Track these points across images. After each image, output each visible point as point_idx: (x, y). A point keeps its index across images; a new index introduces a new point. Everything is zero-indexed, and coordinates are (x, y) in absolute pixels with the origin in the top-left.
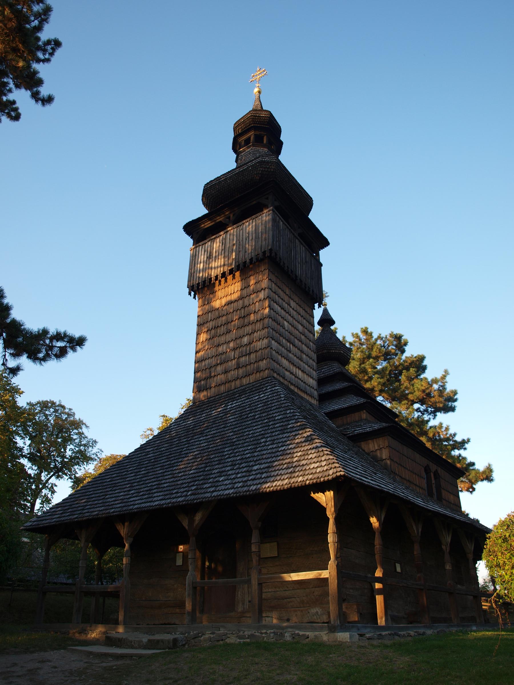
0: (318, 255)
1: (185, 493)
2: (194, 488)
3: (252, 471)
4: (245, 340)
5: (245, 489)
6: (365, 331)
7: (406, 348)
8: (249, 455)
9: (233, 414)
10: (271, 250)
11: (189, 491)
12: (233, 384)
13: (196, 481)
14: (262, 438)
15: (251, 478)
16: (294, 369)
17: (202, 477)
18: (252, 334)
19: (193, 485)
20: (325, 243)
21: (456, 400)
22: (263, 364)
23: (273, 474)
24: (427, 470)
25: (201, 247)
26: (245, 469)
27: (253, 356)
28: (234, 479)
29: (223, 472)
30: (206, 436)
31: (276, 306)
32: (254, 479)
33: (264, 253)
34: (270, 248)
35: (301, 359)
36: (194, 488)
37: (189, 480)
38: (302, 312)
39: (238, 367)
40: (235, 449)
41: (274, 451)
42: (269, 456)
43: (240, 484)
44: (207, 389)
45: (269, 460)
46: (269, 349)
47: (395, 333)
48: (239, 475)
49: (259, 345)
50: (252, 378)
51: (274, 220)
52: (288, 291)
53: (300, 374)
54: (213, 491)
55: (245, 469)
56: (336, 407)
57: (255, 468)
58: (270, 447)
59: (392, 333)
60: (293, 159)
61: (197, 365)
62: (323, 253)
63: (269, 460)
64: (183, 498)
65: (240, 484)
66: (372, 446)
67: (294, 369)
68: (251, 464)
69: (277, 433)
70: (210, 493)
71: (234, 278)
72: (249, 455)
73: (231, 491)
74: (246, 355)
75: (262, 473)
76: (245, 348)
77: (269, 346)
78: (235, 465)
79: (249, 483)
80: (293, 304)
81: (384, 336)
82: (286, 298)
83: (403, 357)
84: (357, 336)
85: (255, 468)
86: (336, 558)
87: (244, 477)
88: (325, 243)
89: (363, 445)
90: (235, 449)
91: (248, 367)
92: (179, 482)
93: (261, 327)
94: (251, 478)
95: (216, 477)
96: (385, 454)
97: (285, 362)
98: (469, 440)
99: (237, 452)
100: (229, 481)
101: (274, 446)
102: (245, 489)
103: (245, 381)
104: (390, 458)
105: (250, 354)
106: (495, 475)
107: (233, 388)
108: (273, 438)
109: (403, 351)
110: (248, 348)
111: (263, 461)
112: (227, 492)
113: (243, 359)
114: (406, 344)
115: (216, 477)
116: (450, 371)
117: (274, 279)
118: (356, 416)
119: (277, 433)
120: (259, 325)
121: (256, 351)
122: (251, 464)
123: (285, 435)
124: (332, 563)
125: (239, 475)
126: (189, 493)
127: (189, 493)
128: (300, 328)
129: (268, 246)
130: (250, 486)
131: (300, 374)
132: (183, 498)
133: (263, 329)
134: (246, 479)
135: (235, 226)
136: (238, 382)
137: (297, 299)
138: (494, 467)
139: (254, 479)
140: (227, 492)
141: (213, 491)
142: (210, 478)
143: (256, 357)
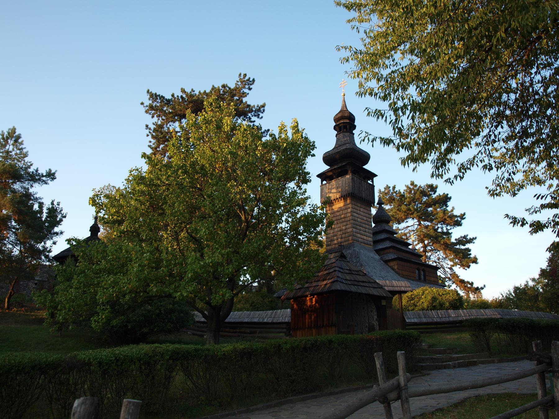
0: (373, 181)
4: (344, 228)
6: (412, 183)
7: (438, 190)
16: (362, 237)
20: (376, 176)
21: (464, 218)
22: (350, 238)
24: (418, 269)
31: (355, 214)
35: (366, 232)
38: (366, 211)
39: (342, 238)
51: (352, 179)
52: (359, 205)
53: (365, 237)
56: (381, 247)
62: (375, 179)
66: (392, 264)
67: (362, 237)
77: (352, 231)
80: (362, 210)
82: (359, 208)
83: (434, 196)
84: (407, 187)
88: (376, 176)
89: (389, 263)
96: (396, 267)
97: (359, 235)
98: (476, 238)
104: (398, 269)
106: (478, 261)
113: (343, 236)
114: (437, 187)
116: (455, 208)
117: (353, 202)
118: (388, 251)
120: (348, 223)
128: (365, 218)
131: (365, 237)
137: (363, 207)
138: (477, 257)
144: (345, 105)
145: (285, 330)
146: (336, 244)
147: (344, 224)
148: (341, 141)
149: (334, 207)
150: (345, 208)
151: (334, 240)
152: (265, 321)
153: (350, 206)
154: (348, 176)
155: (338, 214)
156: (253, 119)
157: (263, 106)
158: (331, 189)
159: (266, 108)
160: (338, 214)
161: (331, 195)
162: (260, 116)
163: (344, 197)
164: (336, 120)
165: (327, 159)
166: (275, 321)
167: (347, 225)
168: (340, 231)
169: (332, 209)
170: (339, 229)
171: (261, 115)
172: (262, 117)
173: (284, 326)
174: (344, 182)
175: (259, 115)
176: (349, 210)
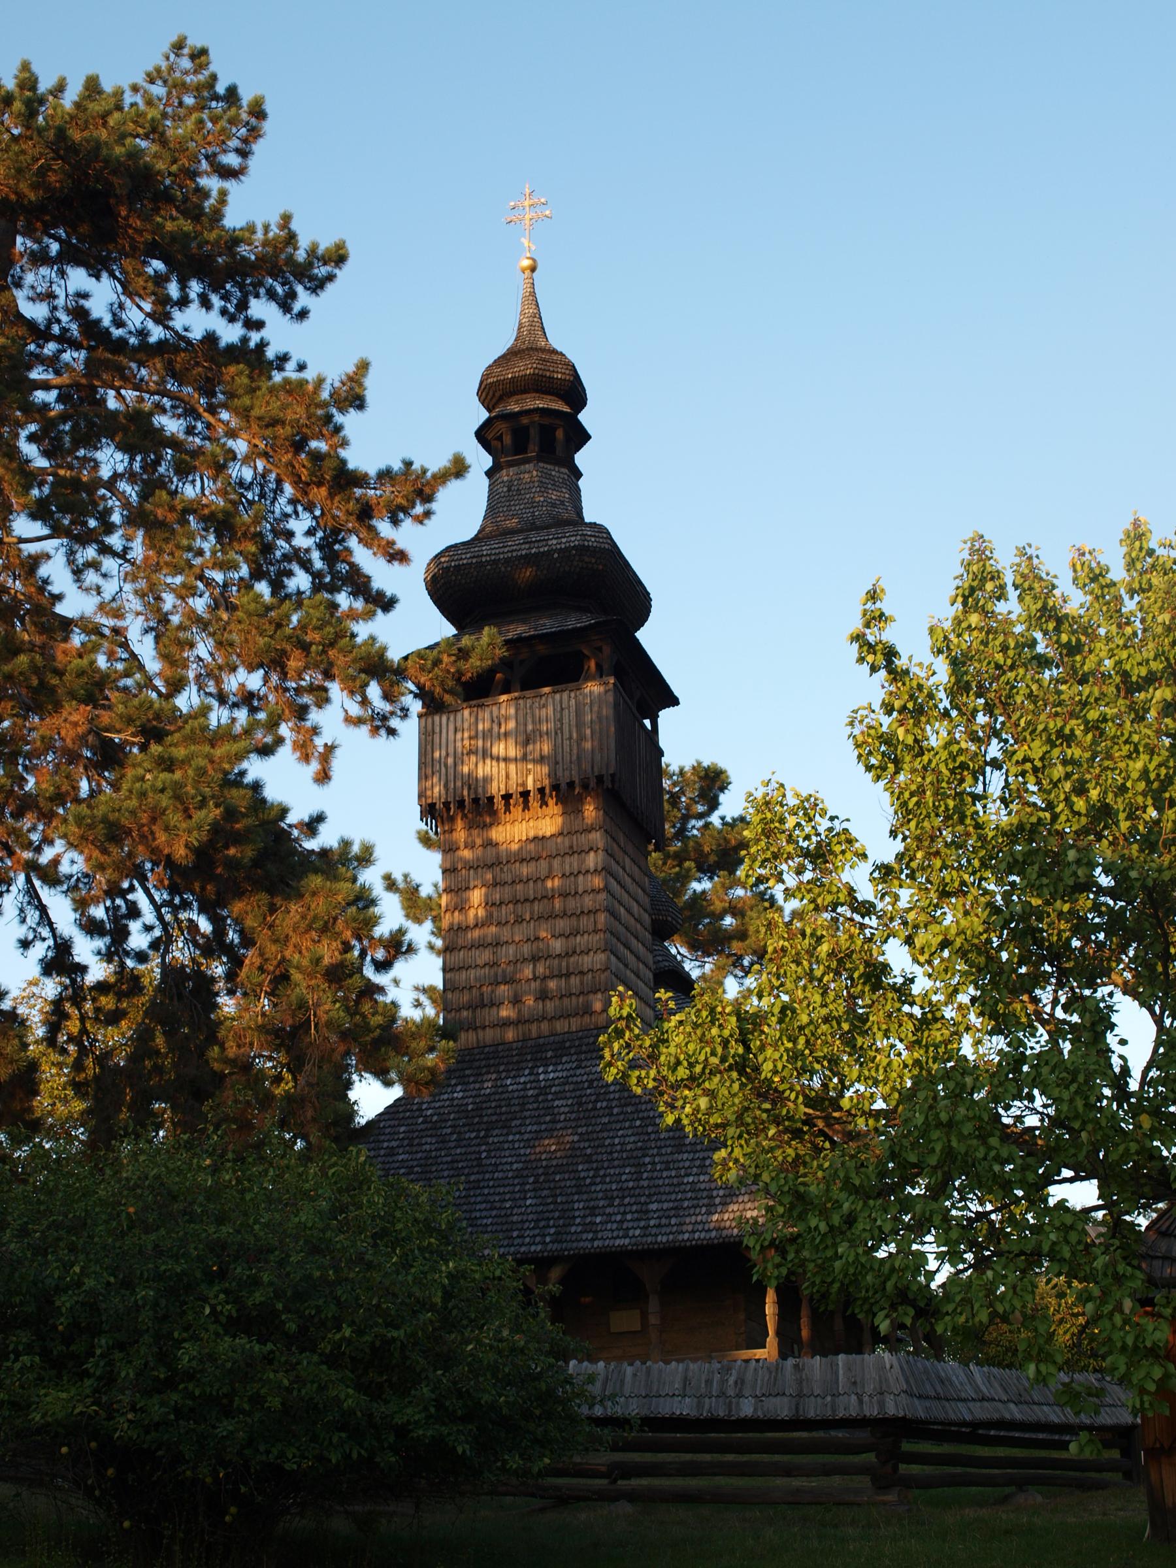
1: (538, 1239)
2: (552, 1231)
3: (647, 1211)
4: (557, 945)
5: (649, 1239)
8: (631, 1184)
9: (558, 1095)
10: (613, 775)
11: (544, 1236)
12: (534, 1027)
13: (548, 1219)
14: (644, 1156)
15: (652, 1223)
17: (557, 1214)
18: (572, 938)
19: (548, 1226)
20: (673, 701)
23: (688, 1220)
25: (444, 718)
26: (634, 1208)
27: (574, 981)
28: (622, 1222)
29: (594, 1208)
30: (520, 1133)
32: (660, 1226)
33: (600, 779)
34: (611, 771)
36: (552, 1231)
37: (535, 1217)
40: (597, 1169)
41: (675, 1181)
42: (667, 1189)
43: (637, 1232)
44: (476, 1029)
45: (673, 1197)
46: (608, 973)
47: (705, 764)
48: (629, 1217)
49: (587, 961)
50: (575, 1024)
54: (593, 1240)
55: (634, 1208)
57: (654, 1206)
58: (665, 1174)
59: (699, 763)
60: (611, 490)
61: (448, 976)
63: (673, 1197)
64: (539, 1247)
65: (637, 1232)
68: (643, 1199)
69: (669, 1150)
70: (589, 1243)
71: (526, 807)
72: (631, 1184)
73: (627, 1241)
74: (560, 976)
75: (669, 1217)
76: (556, 961)
78: (613, 1198)
79: (654, 1231)
81: (677, 770)
85: (654, 1206)
86: (778, 1333)
87: (638, 1220)
88: (673, 701)
90: (597, 1169)
91: (566, 1001)
92: (515, 1218)
93: (591, 928)
94: (652, 1223)
95: (585, 1217)
99: (605, 1176)
100: (615, 1226)
101: (673, 1173)
102: (649, 1239)
103: (561, 1026)
105: (568, 975)
107: (534, 1034)
108: (665, 1158)
109: (714, 805)
110: (564, 964)
111: (664, 1197)
112: (617, 1242)
113: (552, 984)
115: (585, 1217)
119: (669, 1150)
120: (585, 922)
121: (582, 973)
122: (643, 1199)
123: (685, 1156)
124: (772, 1339)
125: (629, 1217)
126: (548, 1239)
127: (548, 1239)
129: (607, 765)
130: (656, 1235)
132: (539, 1247)
133: (596, 931)
134: (642, 1223)
135: (528, 693)
136: (545, 1026)
139: (660, 1226)
140: (617, 1242)
141: (593, 1240)
142: (574, 1217)
143: (582, 983)
144: (533, 324)
145: (871, 1457)
146: (506, 1023)
147: (562, 924)
148: (533, 504)
149: (497, 834)
150: (567, 847)
151: (496, 1004)
152: (747, 1409)
153: (597, 837)
154: (593, 688)
155: (525, 870)
156: (259, 308)
157: (339, 257)
158: (487, 735)
159: (343, 274)
160: (525, 870)
161: (484, 769)
162: (297, 307)
163: (563, 792)
164: (492, 391)
165: (454, 585)
166: (812, 1411)
167: (575, 933)
168: (535, 959)
169: (490, 844)
170: (526, 949)
171: (304, 298)
172: (303, 314)
173: (862, 1436)
174: (569, 717)
175: (292, 295)
176: (591, 860)
